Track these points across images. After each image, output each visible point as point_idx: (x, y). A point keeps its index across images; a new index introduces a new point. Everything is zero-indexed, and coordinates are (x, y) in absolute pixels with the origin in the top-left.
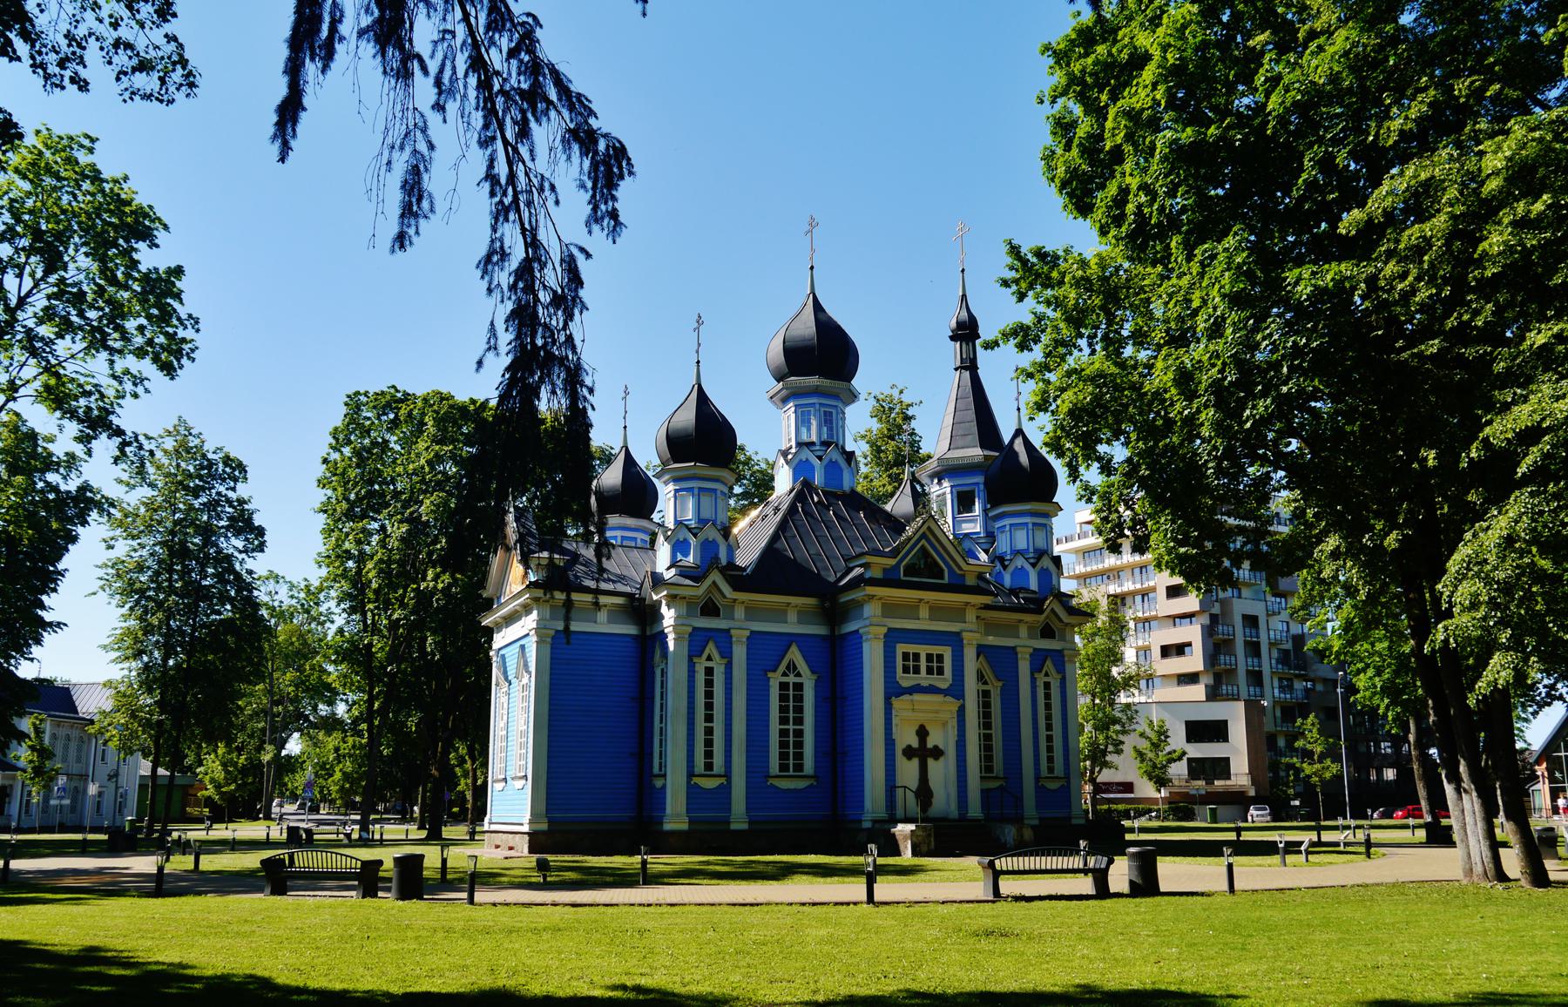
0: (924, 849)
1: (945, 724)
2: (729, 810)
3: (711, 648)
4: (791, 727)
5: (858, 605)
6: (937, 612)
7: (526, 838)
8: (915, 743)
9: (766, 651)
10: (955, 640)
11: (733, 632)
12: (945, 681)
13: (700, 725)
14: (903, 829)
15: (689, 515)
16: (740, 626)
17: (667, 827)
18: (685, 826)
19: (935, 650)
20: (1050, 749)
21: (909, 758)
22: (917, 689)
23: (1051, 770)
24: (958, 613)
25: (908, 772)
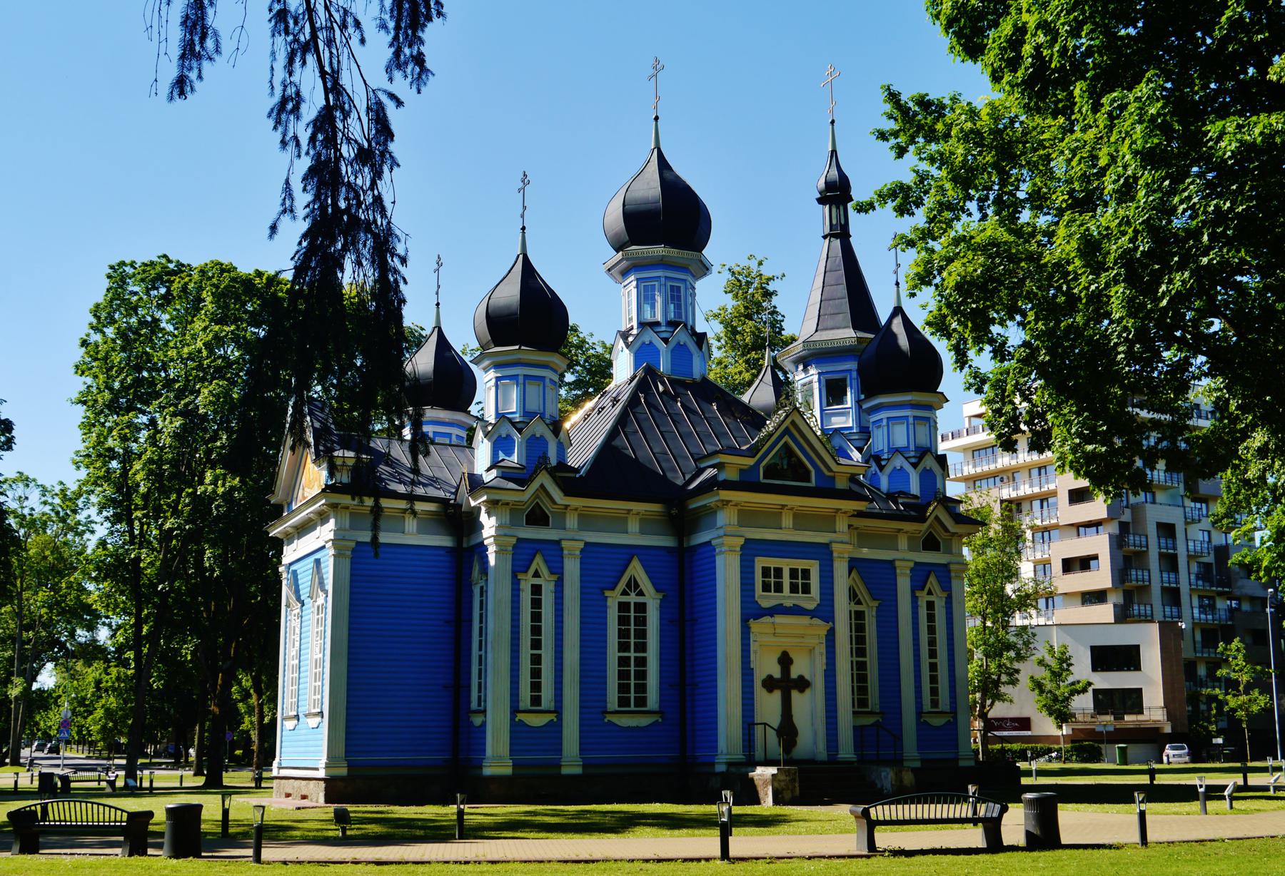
0: (788, 795)
1: (811, 650)
2: (561, 750)
3: (538, 563)
4: (632, 654)
5: (711, 512)
6: (801, 520)
7: (322, 784)
8: (777, 673)
9: (603, 566)
10: (823, 553)
11: (564, 544)
12: (811, 600)
13: (526, 652)
14: (763, 774)
15: (513, 407)
16: (573, 537)
17: (487, 771)
18: (508, 771)
19: (800, 564)
20: (934, 679)
21: (770, 690)
22: (779, 610)
23: (935, 703)
24: (827, 521)
25: (769, 706)
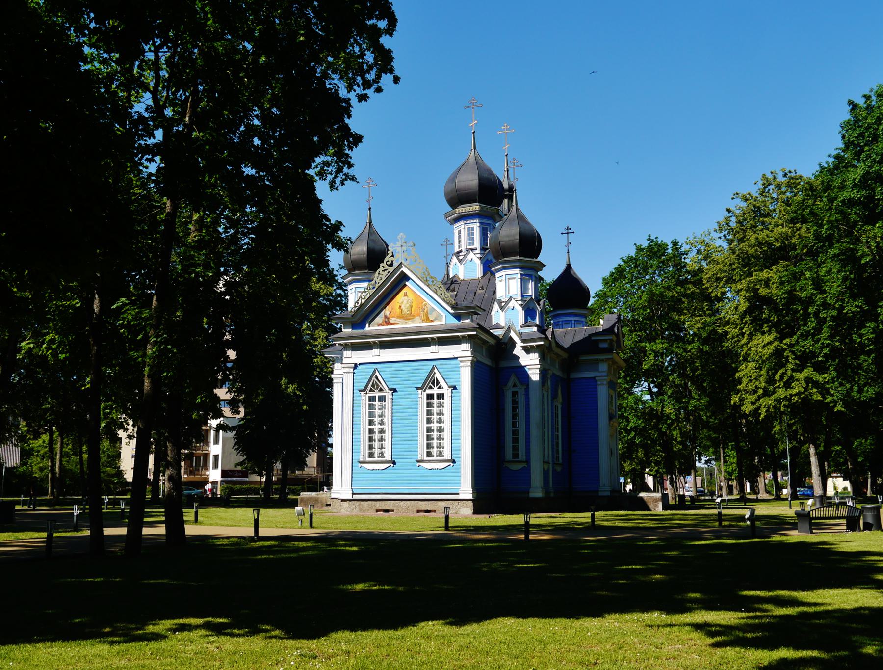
5: (597, 362)
7: (471, 503)
15: (531, 291)
17: (532, 495)
